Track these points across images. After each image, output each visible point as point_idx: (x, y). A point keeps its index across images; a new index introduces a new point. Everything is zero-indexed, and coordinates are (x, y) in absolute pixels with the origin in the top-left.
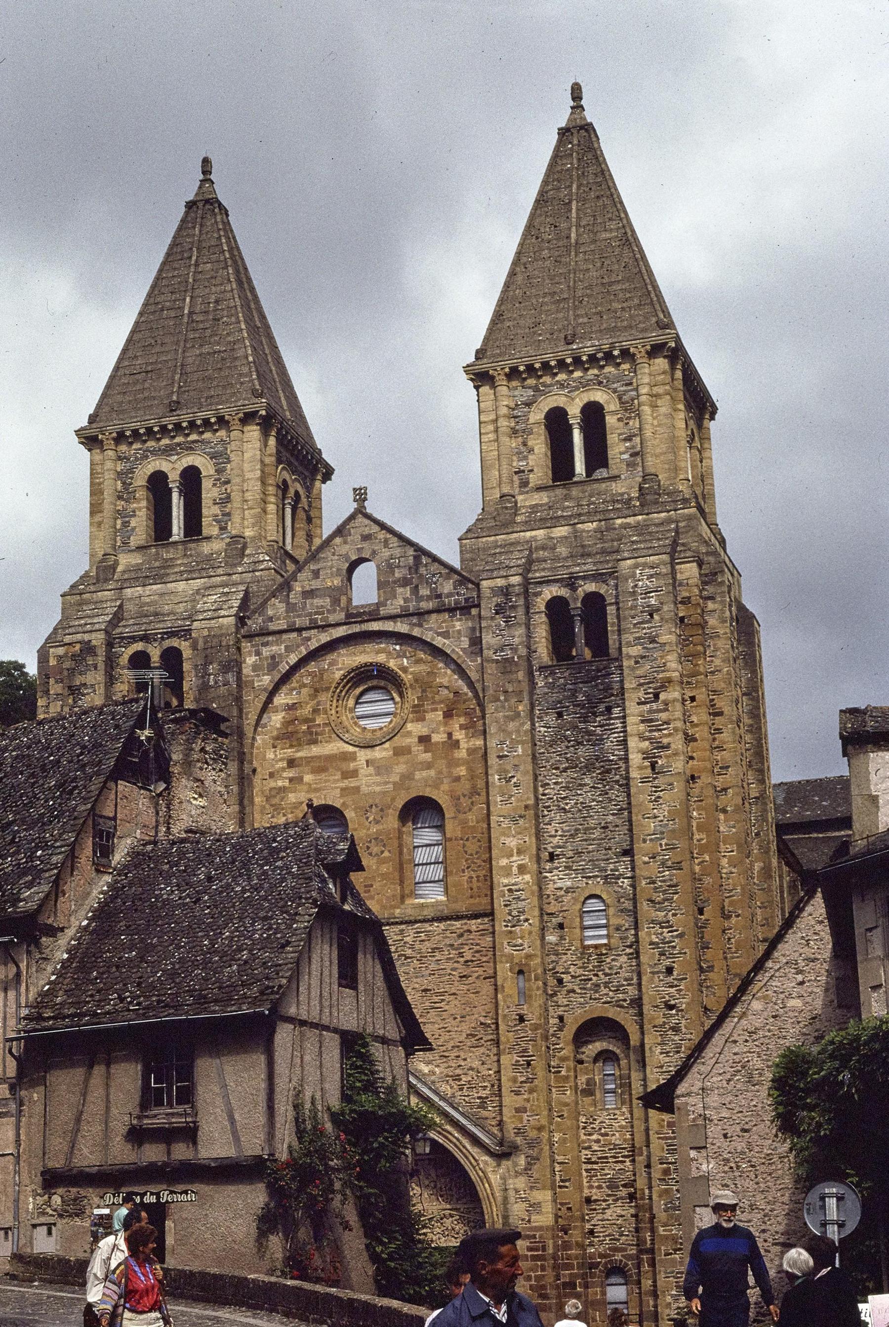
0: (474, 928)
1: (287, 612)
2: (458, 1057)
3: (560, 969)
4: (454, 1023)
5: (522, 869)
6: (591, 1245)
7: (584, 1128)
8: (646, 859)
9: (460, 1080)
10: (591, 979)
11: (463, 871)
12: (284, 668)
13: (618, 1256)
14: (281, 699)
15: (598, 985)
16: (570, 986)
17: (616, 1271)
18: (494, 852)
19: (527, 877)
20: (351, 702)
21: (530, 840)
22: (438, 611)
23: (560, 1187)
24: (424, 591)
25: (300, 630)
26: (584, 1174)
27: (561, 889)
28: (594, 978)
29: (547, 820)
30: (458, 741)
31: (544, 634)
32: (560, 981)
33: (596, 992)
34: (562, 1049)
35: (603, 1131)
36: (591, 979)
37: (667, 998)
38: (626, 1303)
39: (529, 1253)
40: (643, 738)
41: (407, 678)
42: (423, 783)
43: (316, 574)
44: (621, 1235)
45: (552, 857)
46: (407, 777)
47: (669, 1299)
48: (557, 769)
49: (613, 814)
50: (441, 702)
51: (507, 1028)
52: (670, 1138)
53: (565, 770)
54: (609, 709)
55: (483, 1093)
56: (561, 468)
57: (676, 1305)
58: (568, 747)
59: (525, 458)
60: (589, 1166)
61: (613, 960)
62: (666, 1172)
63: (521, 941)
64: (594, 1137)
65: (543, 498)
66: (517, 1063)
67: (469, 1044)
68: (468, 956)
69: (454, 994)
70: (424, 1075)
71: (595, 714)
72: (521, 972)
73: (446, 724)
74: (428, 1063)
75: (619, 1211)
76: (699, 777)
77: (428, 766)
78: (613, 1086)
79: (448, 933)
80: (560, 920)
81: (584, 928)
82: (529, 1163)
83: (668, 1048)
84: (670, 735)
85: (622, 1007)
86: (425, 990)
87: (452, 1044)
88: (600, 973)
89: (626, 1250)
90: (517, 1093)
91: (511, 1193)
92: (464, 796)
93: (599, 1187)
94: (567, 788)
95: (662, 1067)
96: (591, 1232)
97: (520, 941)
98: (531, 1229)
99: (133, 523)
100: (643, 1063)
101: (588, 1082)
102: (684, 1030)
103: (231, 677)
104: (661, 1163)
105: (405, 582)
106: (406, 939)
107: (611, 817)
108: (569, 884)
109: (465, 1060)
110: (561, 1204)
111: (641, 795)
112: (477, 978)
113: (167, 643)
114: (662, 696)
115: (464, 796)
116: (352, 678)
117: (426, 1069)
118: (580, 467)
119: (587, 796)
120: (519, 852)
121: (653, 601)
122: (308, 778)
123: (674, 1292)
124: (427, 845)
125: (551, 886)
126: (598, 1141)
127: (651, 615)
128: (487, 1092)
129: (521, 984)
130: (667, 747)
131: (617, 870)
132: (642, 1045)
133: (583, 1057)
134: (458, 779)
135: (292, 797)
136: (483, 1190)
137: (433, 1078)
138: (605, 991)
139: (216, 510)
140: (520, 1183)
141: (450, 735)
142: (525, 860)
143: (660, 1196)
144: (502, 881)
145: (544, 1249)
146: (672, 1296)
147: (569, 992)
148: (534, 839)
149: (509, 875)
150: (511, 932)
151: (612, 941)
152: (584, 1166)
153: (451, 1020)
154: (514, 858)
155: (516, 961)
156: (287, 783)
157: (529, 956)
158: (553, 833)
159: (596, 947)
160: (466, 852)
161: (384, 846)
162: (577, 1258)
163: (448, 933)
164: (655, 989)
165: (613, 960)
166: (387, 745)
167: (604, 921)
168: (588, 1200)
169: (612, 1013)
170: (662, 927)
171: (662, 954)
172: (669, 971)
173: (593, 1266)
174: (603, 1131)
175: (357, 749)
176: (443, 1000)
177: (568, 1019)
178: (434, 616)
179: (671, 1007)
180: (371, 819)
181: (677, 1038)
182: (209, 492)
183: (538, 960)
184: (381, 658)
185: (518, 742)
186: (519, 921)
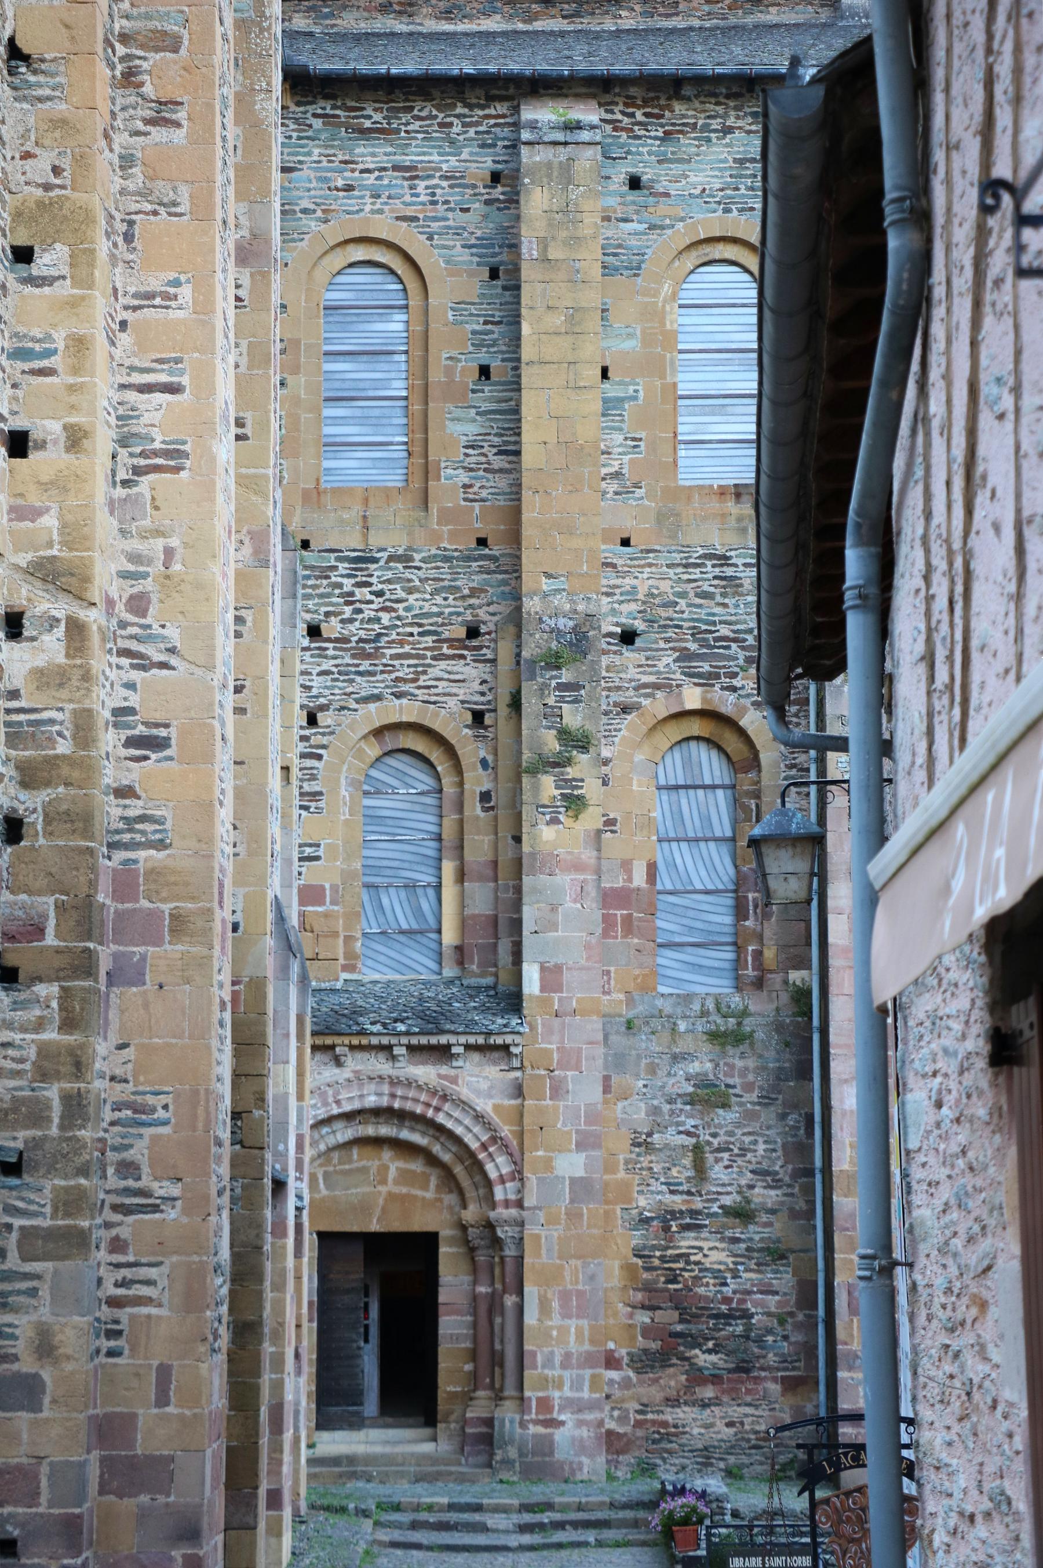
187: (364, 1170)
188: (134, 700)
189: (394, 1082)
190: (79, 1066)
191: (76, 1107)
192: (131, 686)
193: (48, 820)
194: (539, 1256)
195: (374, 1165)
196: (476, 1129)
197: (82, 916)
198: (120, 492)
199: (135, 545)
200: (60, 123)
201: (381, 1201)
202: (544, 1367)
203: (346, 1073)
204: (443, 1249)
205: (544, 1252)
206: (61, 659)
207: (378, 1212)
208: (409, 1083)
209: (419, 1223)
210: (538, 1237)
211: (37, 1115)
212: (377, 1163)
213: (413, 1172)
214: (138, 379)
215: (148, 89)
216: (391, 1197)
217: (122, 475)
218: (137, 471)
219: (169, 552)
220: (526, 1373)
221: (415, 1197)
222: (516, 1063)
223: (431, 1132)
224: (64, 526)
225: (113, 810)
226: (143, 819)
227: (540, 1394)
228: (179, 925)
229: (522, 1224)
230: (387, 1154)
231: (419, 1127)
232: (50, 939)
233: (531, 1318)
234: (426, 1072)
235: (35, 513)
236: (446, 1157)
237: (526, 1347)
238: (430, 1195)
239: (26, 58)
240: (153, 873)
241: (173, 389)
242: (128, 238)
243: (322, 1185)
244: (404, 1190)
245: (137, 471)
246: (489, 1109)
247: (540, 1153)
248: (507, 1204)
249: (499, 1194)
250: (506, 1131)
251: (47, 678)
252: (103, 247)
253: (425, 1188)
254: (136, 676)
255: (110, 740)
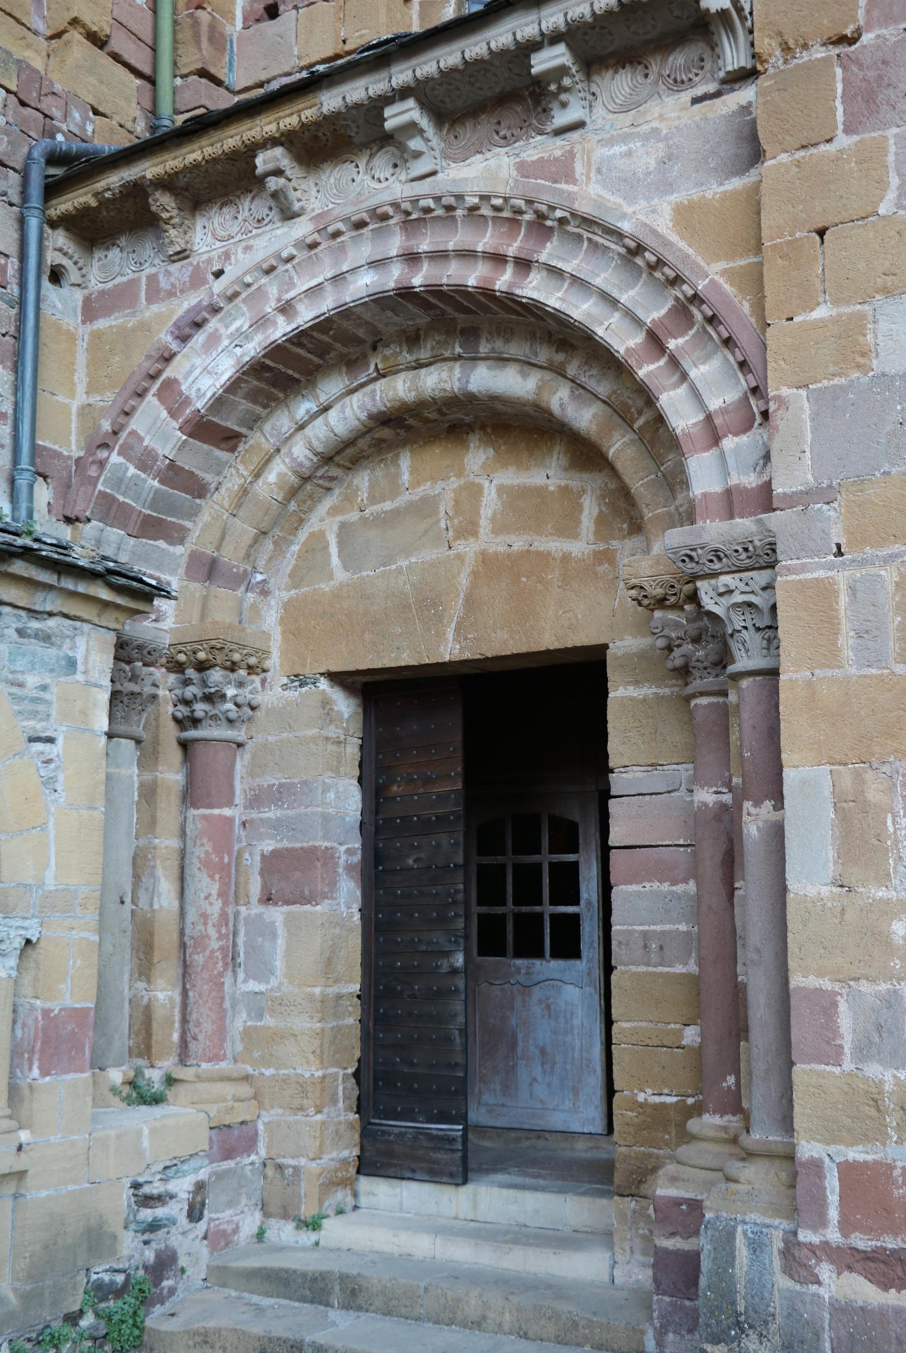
187: (424, 508)
189: (414, 217)
194: (832, 657)
195: (446, 490)
196: (631, 295)
201: (464, 581)
202: (863, 1052)
203: (302, 229)
204: (621, 693)
205: (846, 640)
207: (457, 608)
208: (448, 210)
209: (556, 626)
210: (825, 592)
212: (455, 483)
213: (540, 492)
216: (489, 565)
220: (800, 1070)
221: (544, 557)
222: (734, 57)
223: (544, 354)
227: (855, 1154)
229: (765, 558)
230: (477, 457)
231: (515, 349)
233: (811, 876)
234: (487, 168)
236: (584, 417)
237: (796, 981)
238: (580, 547)
243: (335, 560)
244: (519, 543)
246: (664, 224)
247: (821, 312)
248: (731, 502)
249: (704, 475)
250: (713, 274)
253: (568, 527)
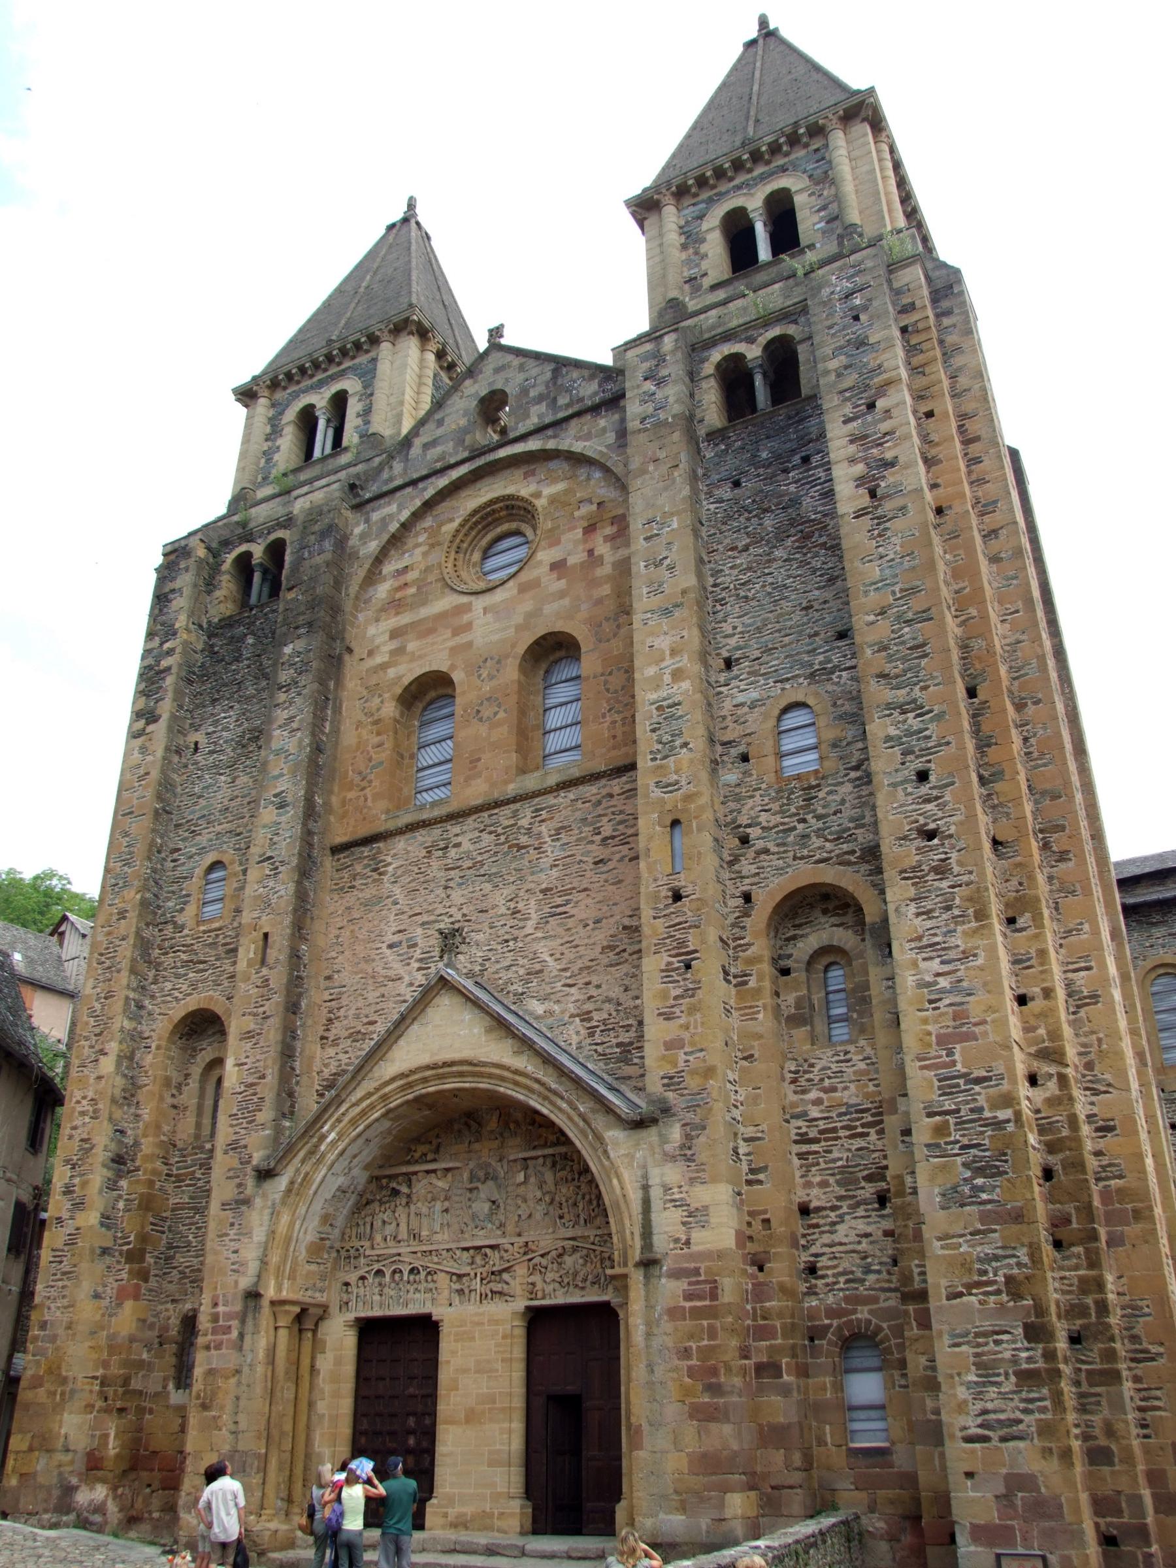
0: (616, 790)
1: (405, 470)
2: (588, 984)
3: (744, 820)
4: (583, 932)
5: (677, 675)
6: (811, 1292)
7: (794, 1081)
8: (872, 618)
9: (590, 1020)
10: (795, 828)
11: (604, 716)
12: (394, 527)
13: (863, 1313)
14: (389, 568)
15: (805, 836)
16: (760, 844)
17: (856, 1341)
18: (637, 663)
19: (686, 685)
20: (477, 556)
21: (693, 636)
22: (578, 414)
23: (749, 1183)
24: (563, 400)
25: (413, 483)
26: (796, 1162)
27: (742, 704)
28: (800, 826)
29: (721, 615)
30: (601, 557)
31: (714, 399)
32: (745, 840)
33: (804, 846)
34: (749, 945)
35: (827, 1082)
36: (795, 828)
37: (922, 821)
38: (882, 1407)
39: (688, 1304)
40: (852, 461)
41: (540, 503)
42: (554, 616)
43: (440, 423)
44: (868, 1270)
45: (729, 664)
46: (536, 613)
47: (962, 1393)
48: (732, 549)
49: (818, 589)
50: (582, 518)
51: (652, 913)
52: (945, 1065)
53: (746, 548)
54: (806, 460)
55: (625, 1037)
56: (741, 252)
57: (979, 1406)
58: (748, 519)
59: (698, 265)
60: (805, 1148)
61: (828, 793)
62: (941, 1130)
63: (674, 772)
64: (813, 1095)
65: (721, 295)
66: (668, 969)
67: (606, 961)
68: (607, 831)
69: (585, 890)
70: (537, 1018)
71: (786, 471)
72: (675, 823)
73: (585, 541)
74: (544, 999)
75: (862, 1226)
76: (950, 507)
77: (562, 594)
78: (843, 1010)
79: (579, 804)
80: (742, 749)
81: (781, 756)
82: (688, 1137)
83: (928, 905)
84: (896, 446)
85: (849, 863)
86: (544, 891)
87: (579, 964)
88: (809, 817)
89: (875, 1300)
90: (668, 1017)
91: (656, 1193)
92: (607, 619)
93: (824, 1184)
94: (749, 569)
95: (920, 938)
96: (812, 1270)
97: (675, 777)
98: (693, 1257)
99: (276, 457)
100: (885, 948)
101: (798, 1004)
102: (956, 869)
103: (328, 545)
104: (929, 1115)
105: (540, 399)
106: (520, 823)
107: (817, 593)
108: (754, 695)
109: (598, 987)
110: (750, 1214)
111: (855, 536)
112: (621, 860)
113: (273, 537)
114: (880, 404)
115: (607, 619)
116: (476, 524)
117: (539, 1008)
118: (764, 252)
119: (779, 574)
120: (673, 652)
121: (858, 302)
122: (411, 646)
123: (972, 1378)
124: (561, 705)
125: (728, 704)
126: (818, 1102)
127: (856, 318)
128: (632, 1034)
129: (677, 844)
130: (891, 464)
131: (830, 661)
132: (885, 920)
133: (789, 963)
134: (599, 602)
135: (392, 673)
136: (611, 1191)
137: (550, 1021)
138: (816, 842)
139: (359, 421)
140: (673, 1174)
141: (591, 552)
142: (685, 661)
143: (932, 1179)
144: (646, 698)
145: (714, 1296)
146: (969, 1385)
147: (758, 853)
148: (696, 632)
149: (658, 687)
150: (660, 767)
151: (827, 764)
152: (797, 1148)
153: (580, 928)
154: (668, 662)
155: (668, 807)
156: (386, 658)
157: (688, 798)
158: (730, 631)
159: (798, 777)
160: (608, 690)
161: (499, 706)
162: (780, 1315)
163: (579, 804)
164: (896, 809)
165: (829, 793)
166: (511, 583)
167: (813, 741)
168: (805, 1210)
169: (829, 875)
170: (904, 712)
171: (905, 753)
172: (923, 776)
173: (813, 1335)
174: (827, 1082)
175: (472, 598)
176: (568, 902)
177: (759, 896)
178: (574, 422)
179: (931, 835)
180: (484, 675)
181: (945, 884)
182: (353, 407)
183: (704, 800)
184: (510, 490)
185: (672, 514)
186: (673, 748)
188: (1095, 1110)
190: (1100, 1285)
191: (1103, 1308)
192: (1092, 1104)
193: (1064, 1168)
197: (1087, 1211)
198: (1072, 1017)
199: (1083, 1039)
200: (1019, 865)
206: (1057, 1092)
211: (1083, 1311)
214: (1071, 967)
215: (1055, 848)
217: (1072, 1010)
218: (1078, 1007)
219: (1100, 1040)
224: (1048, 1033)
225: (1092, 1163)
226: (1110, 1165)
228: (1137, 1215)
232: (1075, 1225)
235: (1033, 1029)
239: (1001, 843)
240: (1119, 1191)
241: (1088, 969)
242: (1057, 909)
245: (1078, 1007)
251: (1051, 1102)
252: (1046, 913)
254: (1094, 1099)
255: (1086, 1130)
